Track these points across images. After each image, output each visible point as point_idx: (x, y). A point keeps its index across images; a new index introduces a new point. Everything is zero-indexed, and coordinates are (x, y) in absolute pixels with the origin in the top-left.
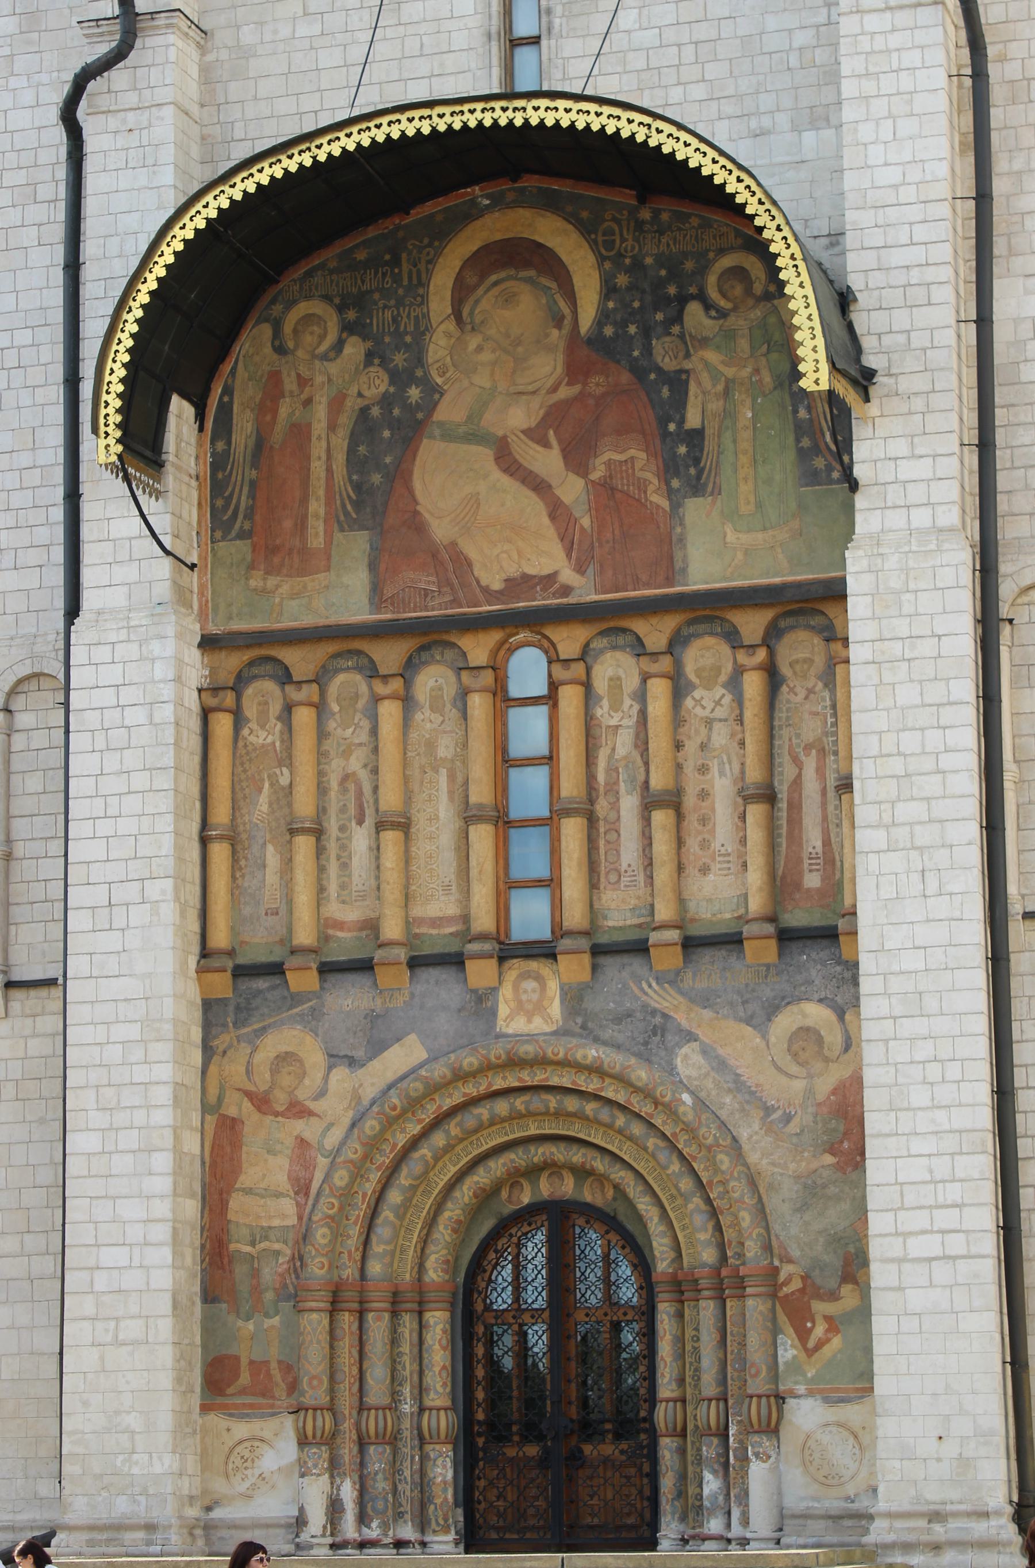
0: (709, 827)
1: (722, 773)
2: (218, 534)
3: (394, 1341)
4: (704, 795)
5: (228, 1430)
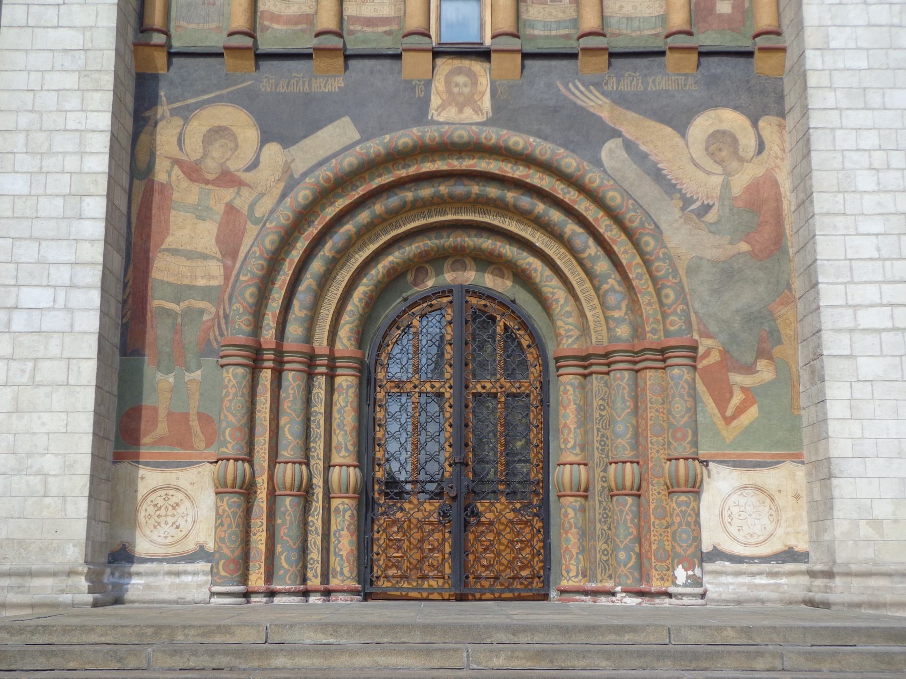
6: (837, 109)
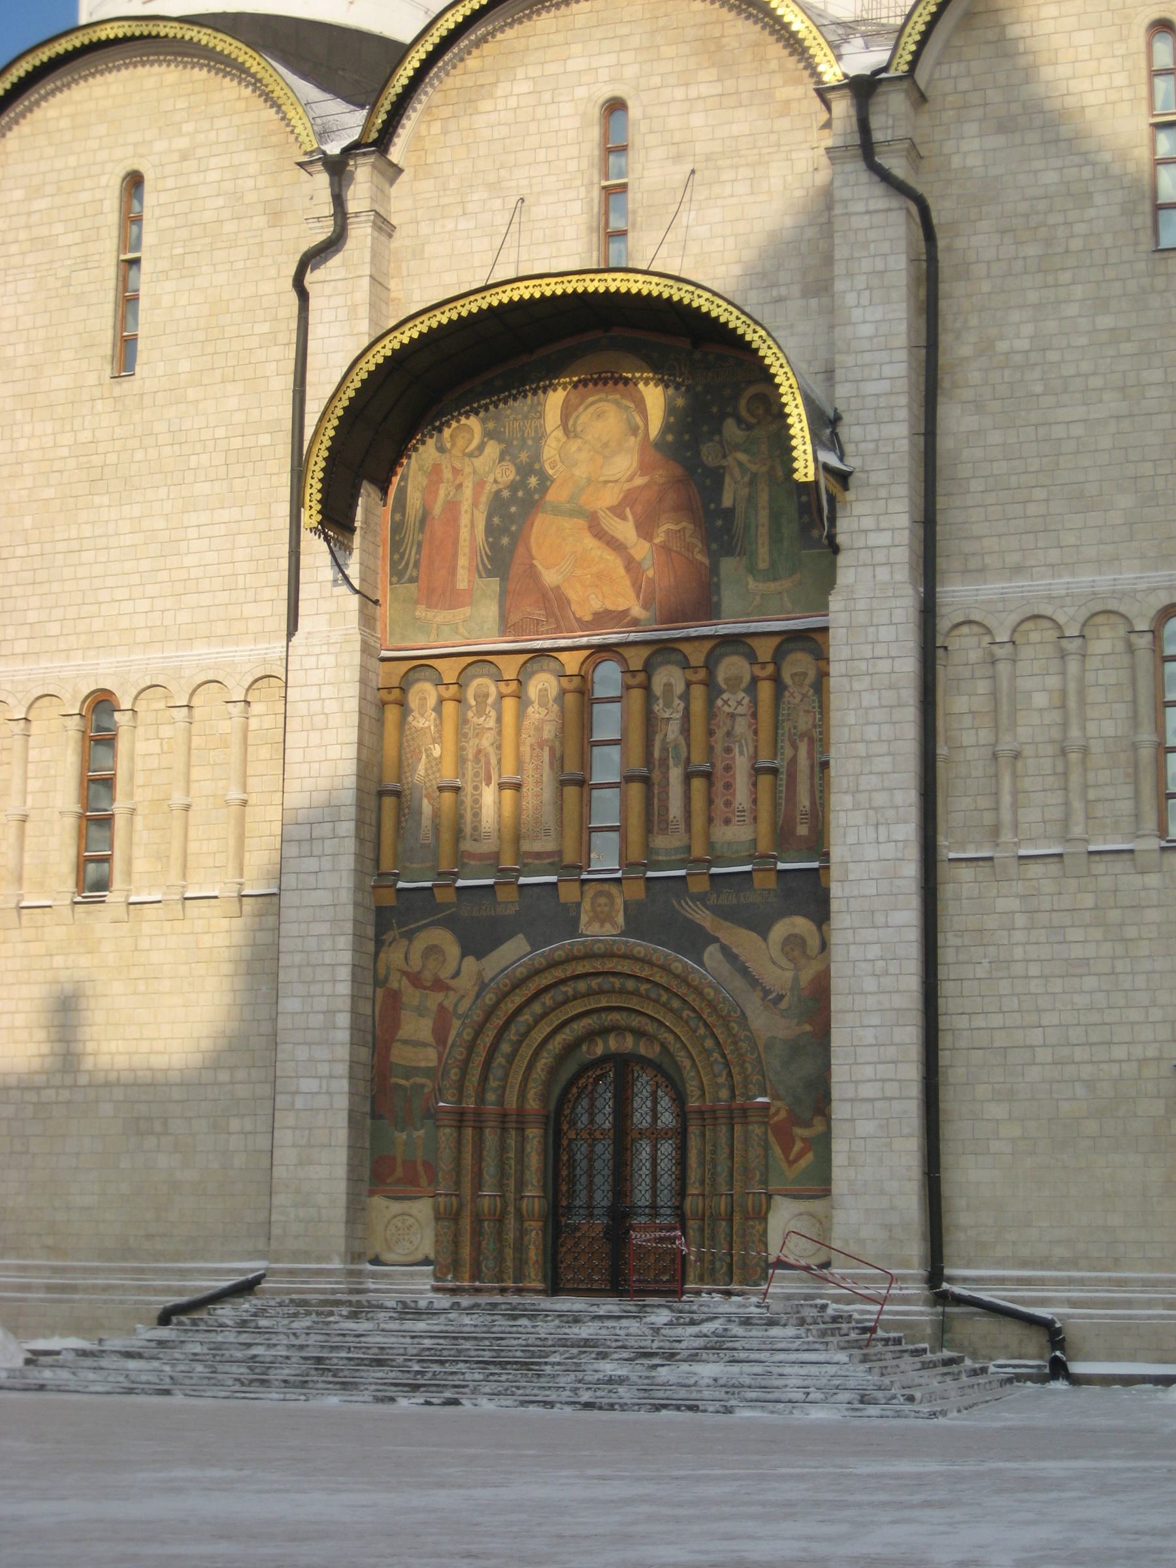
1: (741, 753)
2: (395, 579)
3: (503, 1148)
4: (728, 768)
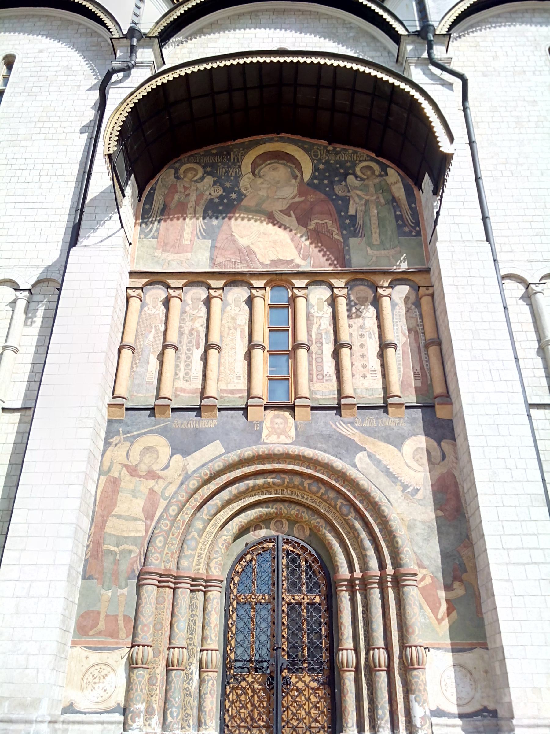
0: (366, 359)
1: (370, 338)
2: (142, 236)
4: (362, 346)
5: (87, 658)
6: (483, 435)
